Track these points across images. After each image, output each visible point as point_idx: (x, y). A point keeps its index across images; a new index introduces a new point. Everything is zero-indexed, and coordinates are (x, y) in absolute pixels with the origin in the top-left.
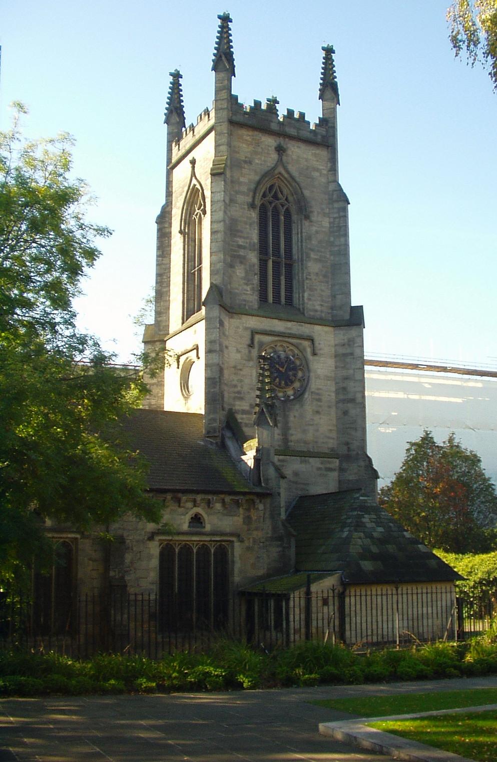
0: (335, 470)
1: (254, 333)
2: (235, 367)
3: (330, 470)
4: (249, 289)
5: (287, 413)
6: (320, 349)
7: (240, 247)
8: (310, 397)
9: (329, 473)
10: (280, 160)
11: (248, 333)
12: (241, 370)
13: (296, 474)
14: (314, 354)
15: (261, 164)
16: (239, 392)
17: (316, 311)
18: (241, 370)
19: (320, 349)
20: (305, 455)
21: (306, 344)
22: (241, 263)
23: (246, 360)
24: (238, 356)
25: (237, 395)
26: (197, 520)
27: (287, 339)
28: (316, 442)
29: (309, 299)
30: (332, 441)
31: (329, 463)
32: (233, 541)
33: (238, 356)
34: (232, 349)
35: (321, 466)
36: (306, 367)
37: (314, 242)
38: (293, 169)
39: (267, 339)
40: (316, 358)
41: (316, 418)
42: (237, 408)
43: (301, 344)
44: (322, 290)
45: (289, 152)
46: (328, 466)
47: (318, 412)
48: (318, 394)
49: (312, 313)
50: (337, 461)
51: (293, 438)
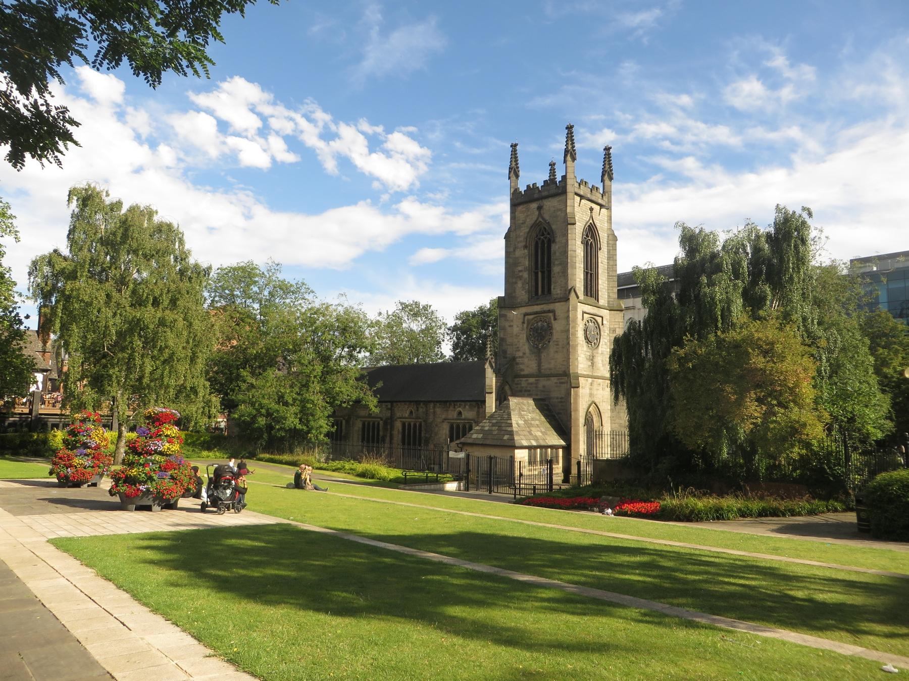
1: (526, 315)
2: (516, 335)
10: (540, 215)
11: (522, 316)
13: (544, 387)
14: (555, 319)
16: (518, 348)
17: (557, 294)
21: (551, 315)
26: (460, 413)
27: (543, 315)
31: (562, 379)
33: (518, 329)
34: (515, 326)
37: (558, 254)
38: (547, 217)
39: (531, 317)
42: (517, 355)
44: (561, 281)
45: (545, 207)
46: (561, 381)
47: (557, 352)
48: (557, 342)
49: (555, 296)
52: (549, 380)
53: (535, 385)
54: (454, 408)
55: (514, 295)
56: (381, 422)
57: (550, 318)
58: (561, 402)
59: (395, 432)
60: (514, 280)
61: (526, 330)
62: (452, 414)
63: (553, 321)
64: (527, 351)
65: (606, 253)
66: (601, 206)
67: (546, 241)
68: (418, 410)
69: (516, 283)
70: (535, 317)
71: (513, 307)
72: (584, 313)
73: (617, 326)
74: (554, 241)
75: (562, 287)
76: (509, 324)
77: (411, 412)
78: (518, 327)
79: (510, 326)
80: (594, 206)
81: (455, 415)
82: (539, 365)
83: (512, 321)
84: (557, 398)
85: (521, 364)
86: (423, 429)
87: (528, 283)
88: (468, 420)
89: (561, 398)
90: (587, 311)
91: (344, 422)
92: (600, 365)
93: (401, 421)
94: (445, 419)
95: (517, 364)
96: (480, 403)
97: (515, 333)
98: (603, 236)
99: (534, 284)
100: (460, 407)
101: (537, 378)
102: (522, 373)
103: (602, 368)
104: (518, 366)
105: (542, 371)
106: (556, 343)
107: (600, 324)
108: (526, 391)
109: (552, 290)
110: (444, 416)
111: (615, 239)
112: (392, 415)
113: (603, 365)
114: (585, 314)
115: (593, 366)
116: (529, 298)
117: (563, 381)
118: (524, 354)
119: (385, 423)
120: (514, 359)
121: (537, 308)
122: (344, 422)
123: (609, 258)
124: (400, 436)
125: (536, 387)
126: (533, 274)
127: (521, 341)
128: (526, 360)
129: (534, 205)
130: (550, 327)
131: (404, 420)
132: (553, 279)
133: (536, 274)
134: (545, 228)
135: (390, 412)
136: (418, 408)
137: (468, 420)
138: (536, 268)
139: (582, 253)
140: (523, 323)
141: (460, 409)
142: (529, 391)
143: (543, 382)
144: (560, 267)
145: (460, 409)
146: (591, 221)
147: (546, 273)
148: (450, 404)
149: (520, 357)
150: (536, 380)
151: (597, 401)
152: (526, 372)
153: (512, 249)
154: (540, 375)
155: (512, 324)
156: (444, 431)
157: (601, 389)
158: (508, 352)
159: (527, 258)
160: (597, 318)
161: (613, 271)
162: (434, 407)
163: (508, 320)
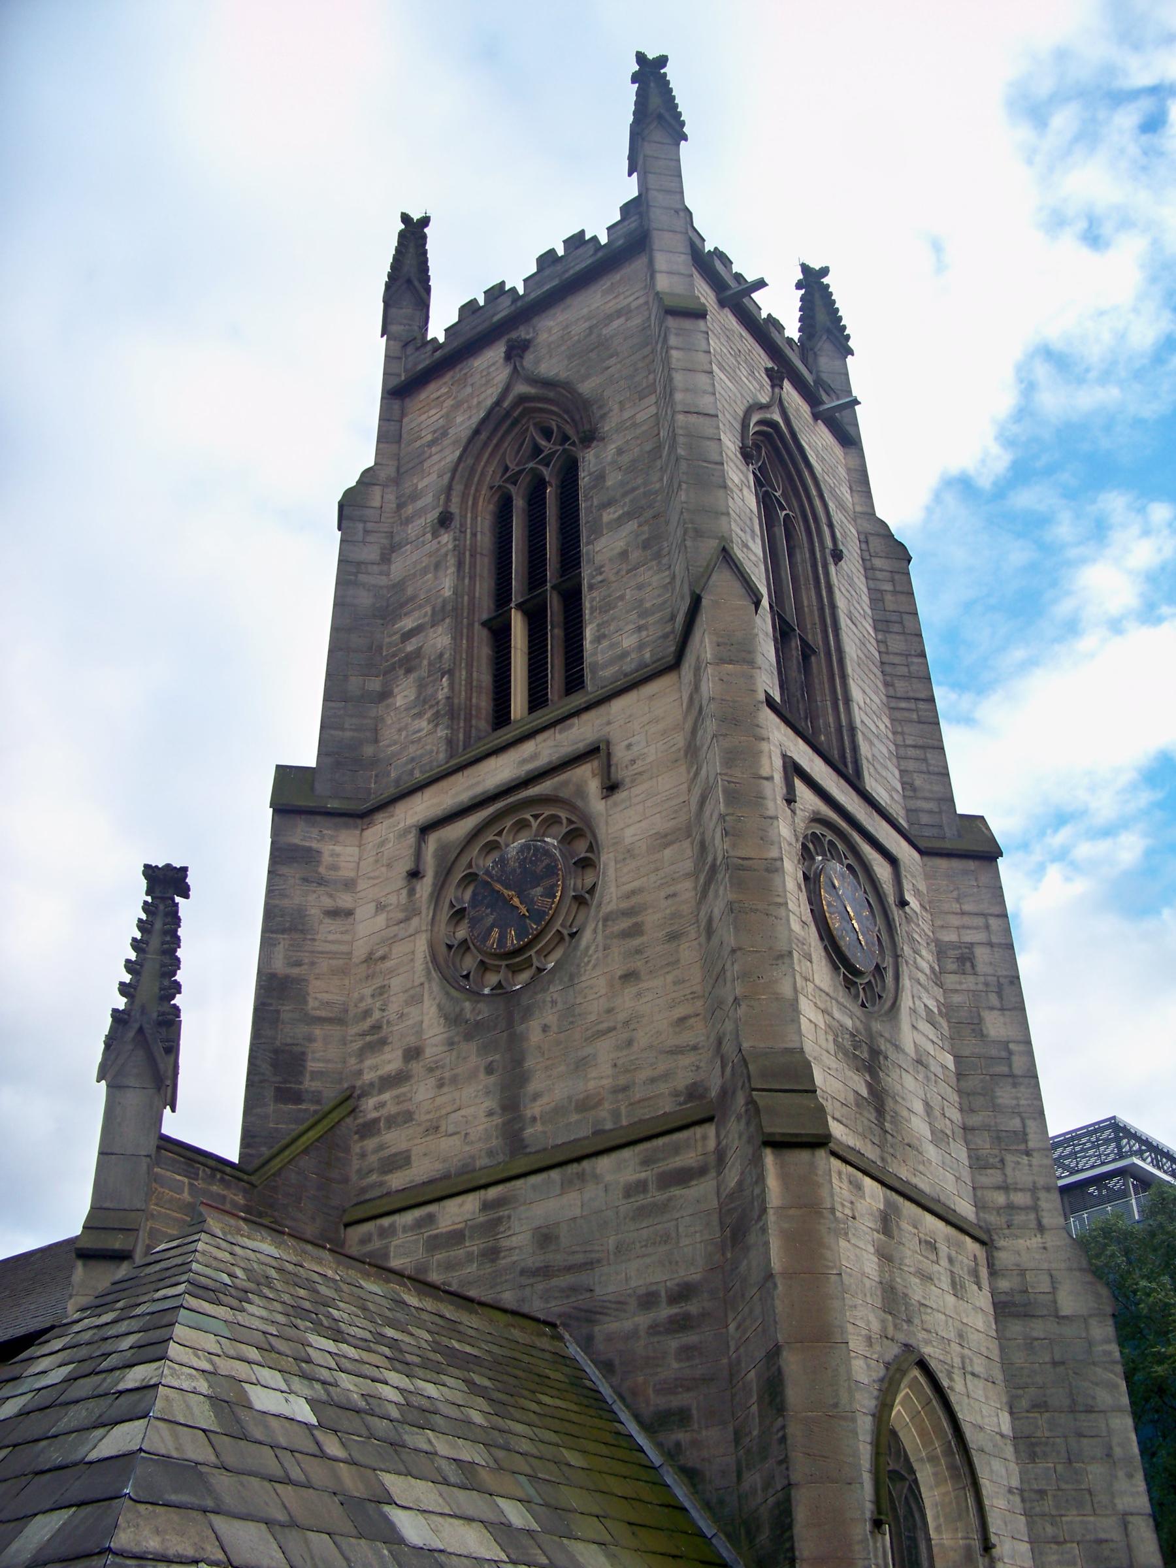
0: (702, 1171)
1: (426, 829)
2: (369, 959)
3: (683, 1177)
4: (424, 724)
5: (521, 1028)
6: (633, 762)
7: (408, 636)
8: (600, 937)
9: (676, 1192)
11: (411, 839)
12: (383, 958)
13: (545, 1238)
14: (611, 788)
15: (470, 417)
16: (376, 1028)
17: (624, 654)
18: (383, 958)
19: (633, 762)
22: (409, 671)
24: (381, 920)
25: (368, 1038)
28: (625, 1089)
29: (598, 639)
30: (686, 1060)
31: (677, 1150)
33: (381, 920)
34: (364, 912)
35: (643, 1175)
37: (613, 479)
40: (620, 796)
41: (627, 1001)
42: (368, 1076)
43: (565, 783)
44: (640, 587)
47: (629, 977)
50: (710, 1130)
51: (534, 1109)
52: (582, 1177)
53: (474, 1246)
55: (368, 750)
57: (581, 792)
58: (681, 1324)
60: (375, 684)
61: (426, 913)
63: (597, 805)
69: (385, 695)
72: (793, 769)
73: (980, 937)
75: (644, 614)
76: (327, 903)
78: (380, 907)
79: (334, 913)
83: (349, 885)
84: (648, 1300)
85: (392, 1122)
87: (450, 672)
89: (684, 1292)
92: (919, 1126)
97: (360, 950)
99: (484, 676)
101: (493, 1193)
102: (396, 1181)
103: (931, 1152)
104: (371, 1144)
106: (625, 924)
109: (588, 645)
113: (939, 1138)
115: (880, 1111)
116: (450, 742)
117: (688, 1159)
118: (413, 1053)
120: (349, 1100)
123: (882, 625)
125: (492, 1254)
126: (482, 636)
127: (396, 983)
128: (422, 1092)
138: (502, 595)
140: (415, 875)
144: (632, 525)
147: (554, 604)
150: (486, 1206)
151: (931, 1352)
152: (421, 1170)
153: (370, 553)
155: (345, 900)
157: (945, 1283)
158: (312, 1065)
159: (452, 561)
161: (909, 677)
163: (322, 882)
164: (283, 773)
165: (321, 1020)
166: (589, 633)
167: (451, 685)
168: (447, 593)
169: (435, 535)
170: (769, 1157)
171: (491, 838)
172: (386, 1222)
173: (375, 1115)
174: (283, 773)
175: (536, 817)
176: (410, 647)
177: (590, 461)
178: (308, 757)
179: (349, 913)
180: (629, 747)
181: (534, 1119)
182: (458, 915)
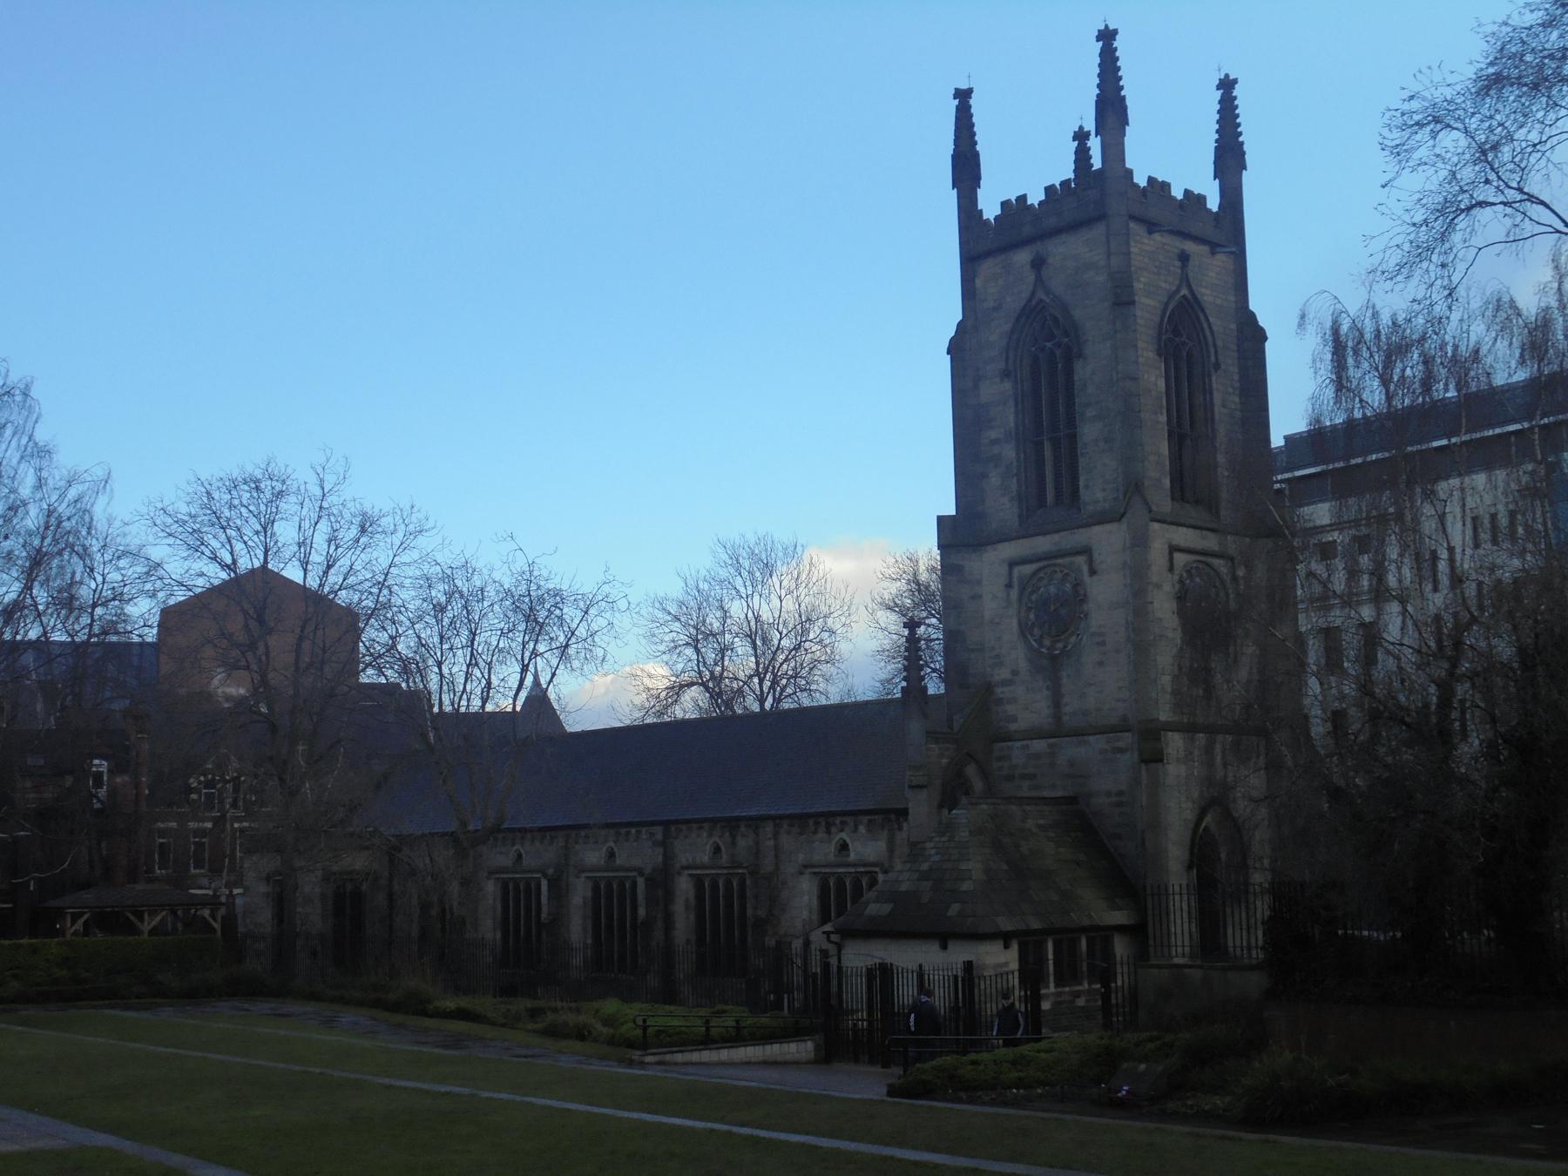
1: (1012, 564)
3: (1121, 750)
7: (994, 442)
9: (1118, 756)
10: (1039, 281)
11: (1004, 570)
12: (997, 623)
14: (1093, 572)
16: (998, 656)
20: (1079, 733)
21: (1081, 560)
23: (1004, 608)
26: (844, 847)
27: (1060, 561)
32: (876, 872)
36: (1084, 599)
39: (1028, 569)
40: (1095, 578)
42: (996, 678)
45: (1050, 261)
47: (1101, 664)
51: (1067, 709)
54: (828, 832)
56: (641, 882)
59: (679, 907)
62: (823, 850)
63: (1087, 579)
64: (1023, 665)
65: (1236, 377)
66: (1214, 247)
67: (1058, 352)
68: (734, 843)
69: (984, 476)
70: (1044, 567)
71: (979, 543)
72: (1173, 549)
74: (1080, 355)
77: (717, 850)
80: (1190, 246)
81: (831, 849)
82: (1057, 702)
84: (1109, 794)
86: (749, 893)
88: (864, 865)
89: (1120, 793)
90: (1183, 544)
91: (544, 883)
93: (690, 875)
94: (806, 867)
95: (999, 702)
96: (893, 817)
98: (1221, 326)
100: (842, 831)
101: (1053, 740)
102: (1013, 727)
105: (1065, 718)
107: (1228, 579)
108: (1024, 777)
109: (1082, 491)
110: (801, 857)
111: (1260, 336)
112: (668, 857)
114: (1177, 556)
116: (1020, 516)
117: (1120, 744)
118: (1015, 673)
119: (650, 881)
120: (989, 688)
121: (1043, 544)
122: (544, 883)
124: (692, 917)
129: (1023, 257)
130: (1078, 598)
131: (699, 872)
132: (1082, 462)
133: (1039, 445)
134: (1056, 320)
135: (661, 850)
136: (733, 837)
137: (864, 865)
139: (1162, 384)
140: (1009, 586)
141: (843, 835)
142: (1032, 777)
143: (1071, 750)
145: (845, 837)
146: (1184, 291)
148: (817, 824)
149: (1005, 683)
150: (1051, 746)
154: (1058, 730)
156: (806, 898)
159: (1011, 403)
160: (1216, 562)
162: (776, 836)
164: (941, 519)
165: (973, 650)
166: (1081, 483)
167: (1018, 481)
168: (1012, 425)
169: (1002, 381)
170: (1143, 766)
171: (1042, 575)
172: (1010, 744)
173: (1001, 696)
174: (941, 519)
175: (1062, 572)
176: (996, 450)
177: (1082, 371)
178: (950, 509)
179: (981, 597)
180: (1099, 554)
181: (1066, 714)
182: (1030, 609)
